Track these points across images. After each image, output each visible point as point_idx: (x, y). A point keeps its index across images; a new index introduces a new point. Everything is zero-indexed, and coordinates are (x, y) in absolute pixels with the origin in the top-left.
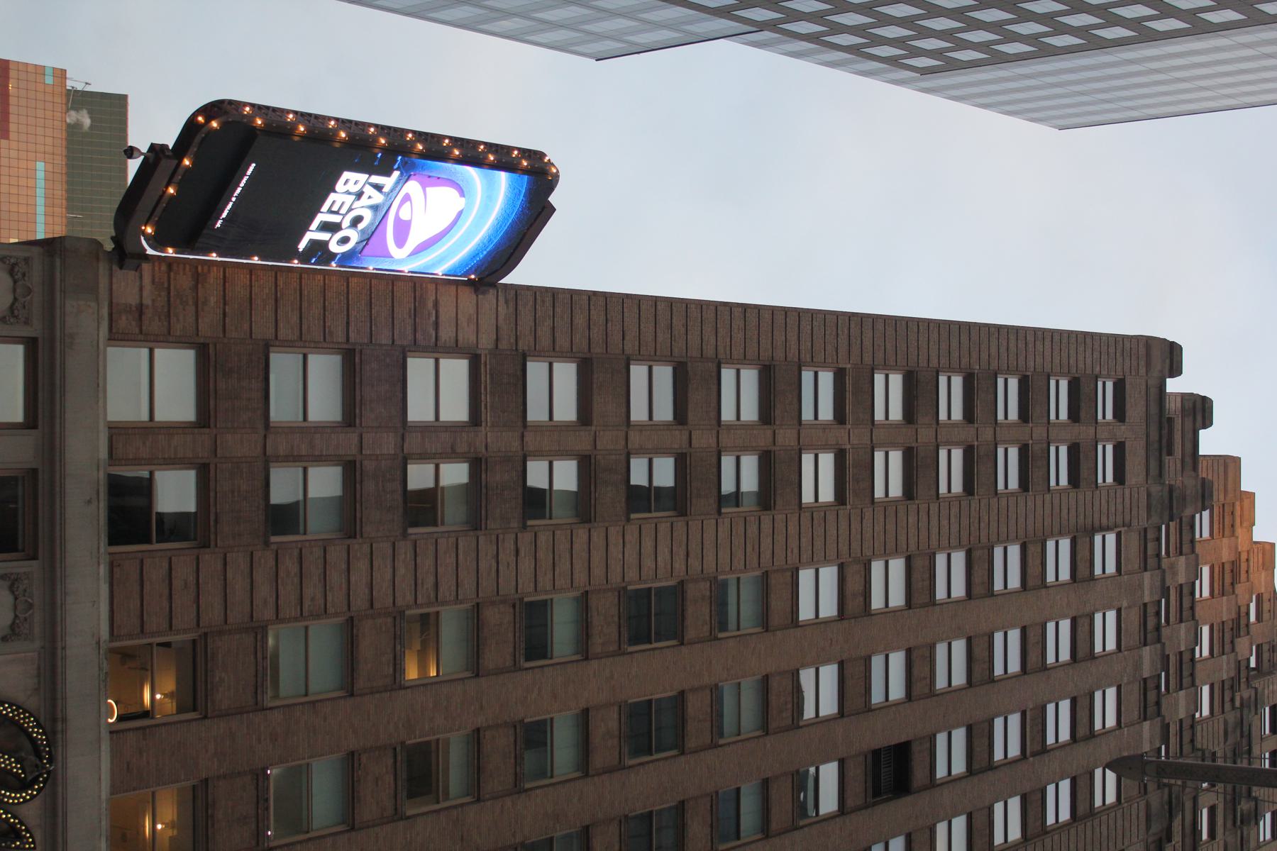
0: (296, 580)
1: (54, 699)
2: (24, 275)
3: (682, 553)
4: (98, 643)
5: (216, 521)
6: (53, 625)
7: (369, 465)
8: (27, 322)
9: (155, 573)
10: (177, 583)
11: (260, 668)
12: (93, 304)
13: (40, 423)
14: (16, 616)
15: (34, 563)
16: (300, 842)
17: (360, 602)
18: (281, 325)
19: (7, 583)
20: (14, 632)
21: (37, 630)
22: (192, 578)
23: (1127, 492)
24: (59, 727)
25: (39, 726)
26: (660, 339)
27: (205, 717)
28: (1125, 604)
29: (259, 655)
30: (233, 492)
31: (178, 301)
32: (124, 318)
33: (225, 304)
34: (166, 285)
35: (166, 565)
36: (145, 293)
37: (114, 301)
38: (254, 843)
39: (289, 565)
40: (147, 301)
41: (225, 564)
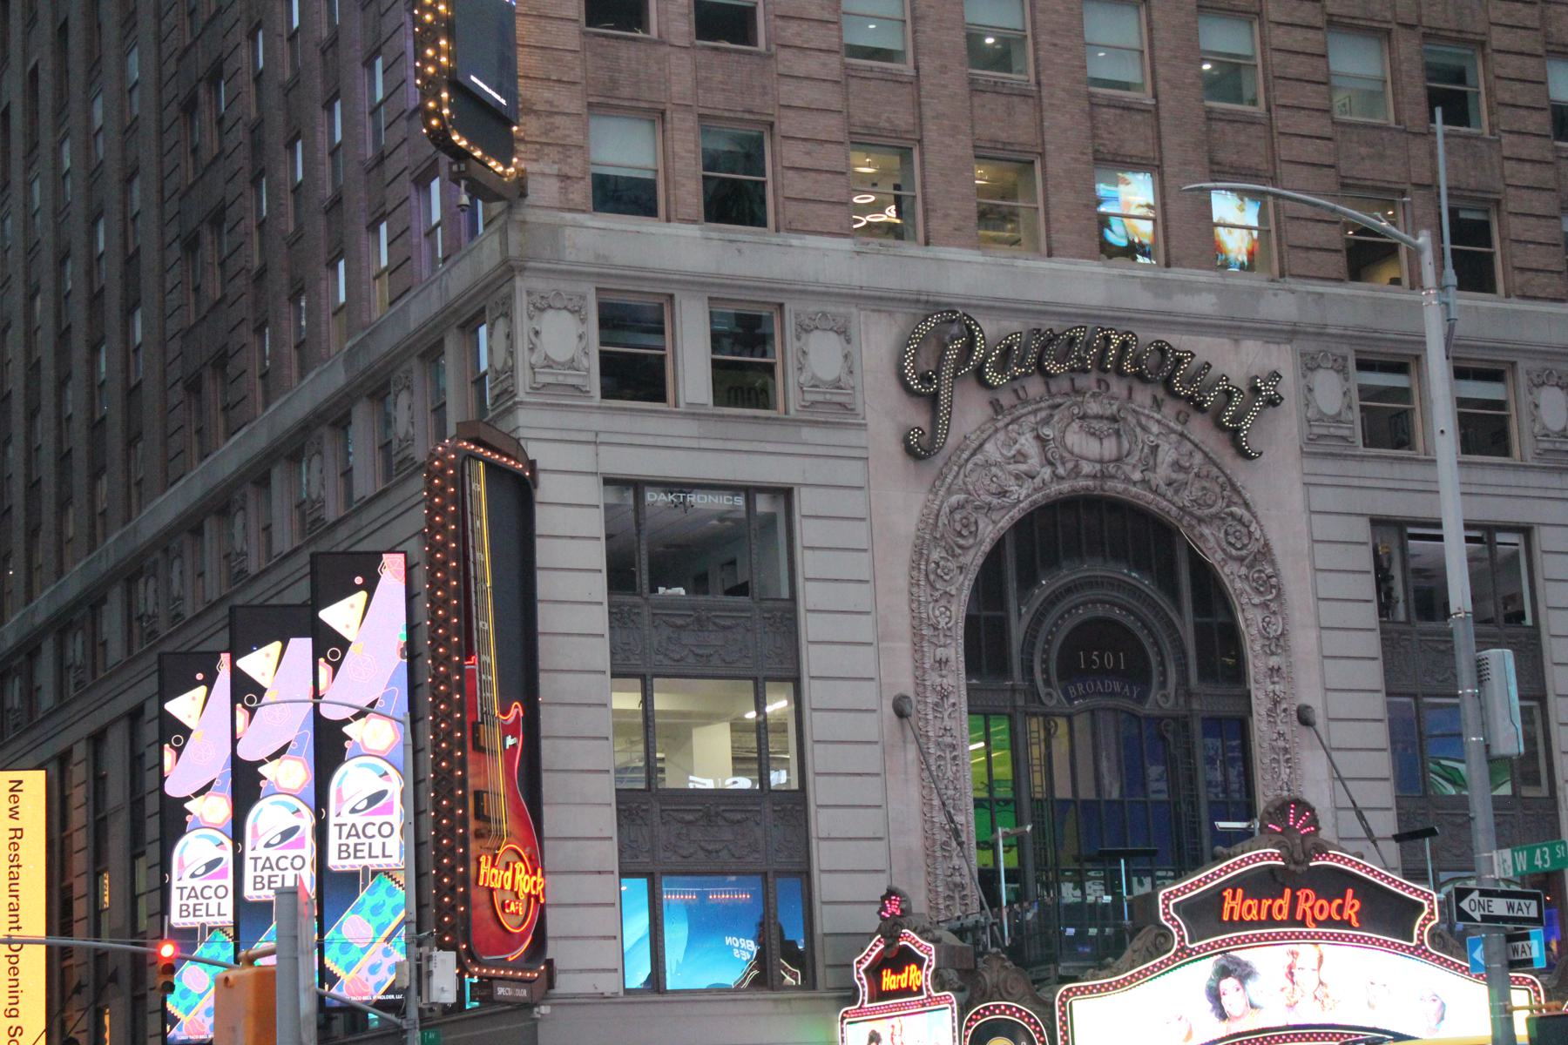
0: (805, 25)
1: (900, 300)
2: (542, 297)
4: (858, 253)
5: (751, 112)
6: (839, 295)
8: (583, 297)
9: (797, 185)
10: (806, 162)
11: (880, 75)
12: (568, 231)
13: (669, 291)
14: (831, 329)
15: (787, 307)
16: (1036, 50)
18: (564, 14)
19: (804, 336)
20: (843, 332)
21: (842, 310)
22: (801, 146)
24: (923, 298)
25: (926, 320)
27: (920, 141)
29: (868, 75)
30: (724, 90)
31: (551, 134)
32: (571, 196)
33: (549, 79)
34: (538, 146)
35: (790, 174)
36: (547, 170)
37: (558, 205)
38: (1030, 101)
39: (790, 31)
40: (554, 169)
41: (789, 107)
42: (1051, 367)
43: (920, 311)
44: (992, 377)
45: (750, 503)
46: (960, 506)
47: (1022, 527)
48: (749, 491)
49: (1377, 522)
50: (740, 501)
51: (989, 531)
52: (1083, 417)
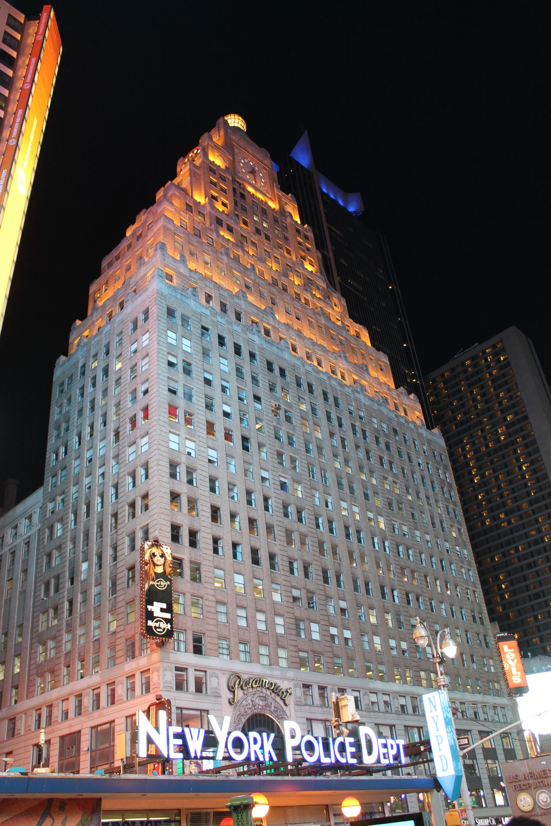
3: (206, 503)
7: (192, 591)
9: (210, 646)
10: (211, 641)
17: (213, 599)
20: (217, 677)
22: (210, 638)
23: (193, 317)
26: (166, 497)
28: (217, 331)
42: (254, 686)
43: (231, 673)
44: (244, 688)
45: (201, 713)
46: (239, 715)
47: (248, 719)
48: (201, 710)
49: (307, 719)
50: (199, 713)
51: (244, 720)
52: (259, 696)
